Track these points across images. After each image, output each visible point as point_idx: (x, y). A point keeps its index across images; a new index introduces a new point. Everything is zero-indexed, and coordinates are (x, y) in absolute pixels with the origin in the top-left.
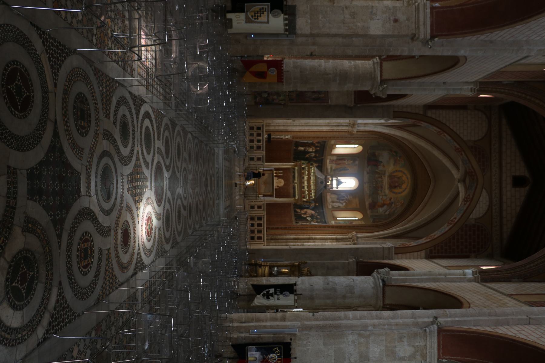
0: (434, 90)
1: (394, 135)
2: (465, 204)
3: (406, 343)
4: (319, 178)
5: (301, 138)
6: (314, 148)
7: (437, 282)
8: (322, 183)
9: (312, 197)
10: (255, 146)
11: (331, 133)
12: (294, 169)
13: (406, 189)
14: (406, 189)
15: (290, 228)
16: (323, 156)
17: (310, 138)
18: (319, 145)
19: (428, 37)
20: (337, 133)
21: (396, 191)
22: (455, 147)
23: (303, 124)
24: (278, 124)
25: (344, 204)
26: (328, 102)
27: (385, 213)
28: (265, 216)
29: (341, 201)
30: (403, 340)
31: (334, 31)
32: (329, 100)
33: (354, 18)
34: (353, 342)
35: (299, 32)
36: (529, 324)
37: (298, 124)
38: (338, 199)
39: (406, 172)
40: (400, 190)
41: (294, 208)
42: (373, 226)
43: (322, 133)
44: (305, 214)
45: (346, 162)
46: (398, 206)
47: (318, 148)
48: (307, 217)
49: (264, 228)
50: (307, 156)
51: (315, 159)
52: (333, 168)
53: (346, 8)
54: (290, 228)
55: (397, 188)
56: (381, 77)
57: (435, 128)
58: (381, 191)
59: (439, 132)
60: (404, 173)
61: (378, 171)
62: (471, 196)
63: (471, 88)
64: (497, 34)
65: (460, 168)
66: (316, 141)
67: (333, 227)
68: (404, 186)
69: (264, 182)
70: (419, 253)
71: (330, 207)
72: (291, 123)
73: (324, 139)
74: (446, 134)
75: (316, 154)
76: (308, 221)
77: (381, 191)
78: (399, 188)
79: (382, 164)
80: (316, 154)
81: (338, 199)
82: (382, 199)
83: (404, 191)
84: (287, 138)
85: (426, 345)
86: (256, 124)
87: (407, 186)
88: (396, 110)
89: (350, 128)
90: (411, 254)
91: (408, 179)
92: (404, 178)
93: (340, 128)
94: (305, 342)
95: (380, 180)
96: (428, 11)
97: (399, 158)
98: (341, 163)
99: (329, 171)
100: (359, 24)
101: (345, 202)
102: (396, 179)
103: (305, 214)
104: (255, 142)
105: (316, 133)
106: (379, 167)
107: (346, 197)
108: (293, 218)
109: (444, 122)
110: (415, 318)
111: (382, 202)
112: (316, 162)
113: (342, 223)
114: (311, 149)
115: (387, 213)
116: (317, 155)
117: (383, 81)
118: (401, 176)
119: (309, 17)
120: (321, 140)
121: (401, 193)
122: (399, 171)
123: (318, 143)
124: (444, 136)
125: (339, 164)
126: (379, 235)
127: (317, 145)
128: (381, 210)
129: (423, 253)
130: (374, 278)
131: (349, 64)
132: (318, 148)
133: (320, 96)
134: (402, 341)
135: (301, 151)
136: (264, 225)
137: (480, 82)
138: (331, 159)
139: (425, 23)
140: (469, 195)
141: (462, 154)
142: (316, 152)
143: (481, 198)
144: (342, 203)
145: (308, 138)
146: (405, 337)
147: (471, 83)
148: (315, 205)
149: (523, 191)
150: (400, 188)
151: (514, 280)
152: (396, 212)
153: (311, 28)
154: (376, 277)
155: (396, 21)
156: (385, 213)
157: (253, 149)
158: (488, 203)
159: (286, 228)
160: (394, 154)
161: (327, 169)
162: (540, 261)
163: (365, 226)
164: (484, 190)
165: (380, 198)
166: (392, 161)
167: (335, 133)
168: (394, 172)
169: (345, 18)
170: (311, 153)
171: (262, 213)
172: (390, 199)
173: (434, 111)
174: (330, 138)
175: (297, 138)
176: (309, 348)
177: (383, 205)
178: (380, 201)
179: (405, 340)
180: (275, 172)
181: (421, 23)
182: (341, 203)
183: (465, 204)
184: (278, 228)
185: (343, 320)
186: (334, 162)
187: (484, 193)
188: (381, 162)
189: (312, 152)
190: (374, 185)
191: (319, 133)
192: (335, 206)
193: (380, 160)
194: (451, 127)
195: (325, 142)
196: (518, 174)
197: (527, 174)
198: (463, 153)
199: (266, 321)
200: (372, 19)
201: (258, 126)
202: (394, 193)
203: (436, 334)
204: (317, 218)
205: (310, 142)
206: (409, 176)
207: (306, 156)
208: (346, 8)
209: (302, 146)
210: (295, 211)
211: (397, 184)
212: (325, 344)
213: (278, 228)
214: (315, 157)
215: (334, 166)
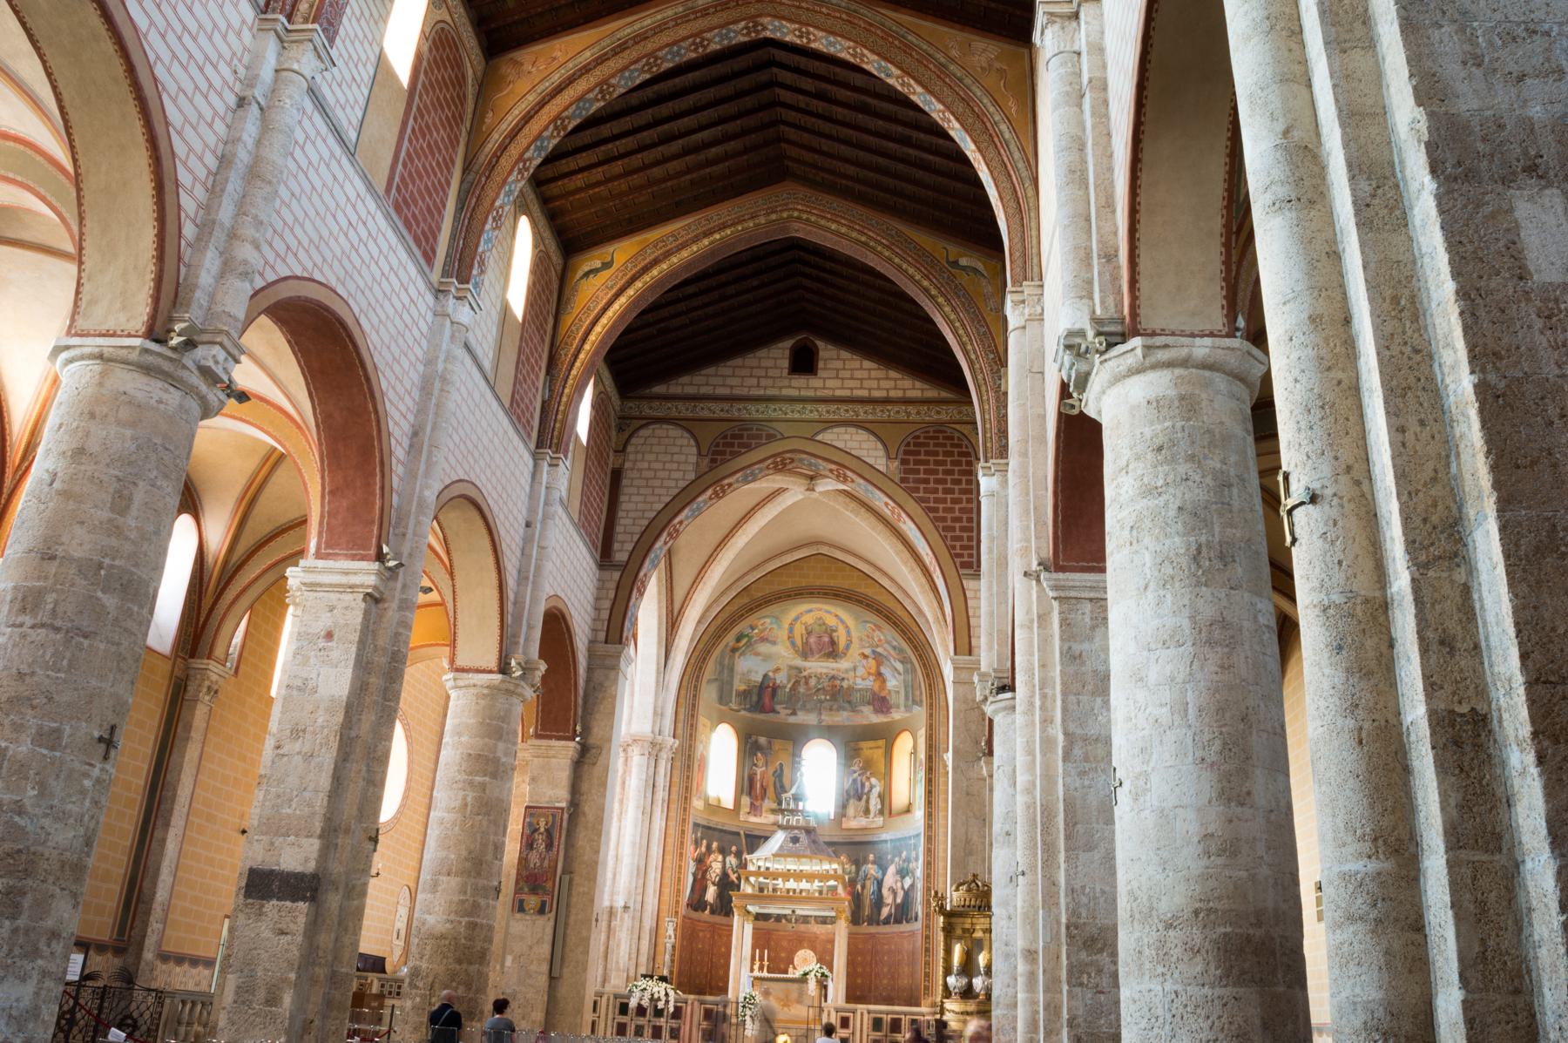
0: (543, 548)
1: (692, 640)
2: (853, 481)
3: (1086, 646)
4: (781, 847)
5: (679, 891)
6: (712, 857)
7: (1006, 558)
8: (795, 840)
9: (835, 870)
10: (674, 1023)
11: (673, 806)
12: (759, 917)
15: (927, 937)
17: (680, 867)
18: (705, 842)
19: (376, 566)
20: (675, 789)
22: (710, 499)
23: (641, 881)
24: (634, 956)
25: (873, 780)
26: (562, 809)
28: (872, 1007)
29: (866, 790)
30: (1077, 653)
31: (325, 781)
32: (557, 805)
33: (304, 731)
34: (1082, 774)
35: (311, 867)
36: (1042, 373)
37: (639, 898)
38: (860, 799)
40: (841, 628)
41: (878, 924)
42: (931, 705)
43: (671, 831)
44: (895, 893)
45: (759, 771)
47: (715, 845)
48: (903, 888)
49: (905, 1014)
52: (775, 806)
53: (278, 747)
54: (927, 937)
56: (491, 672)
57: (659, 544)
59: (670, 534)
62: (833, 467)
63: (550, 465)
64: (396, 423)
65: (777, 486)
66: (691, 852)
67: (929, 816)
68: (831, 621)
69: (784, 1006)
70: (969, 594)
71: (880, 821)
72: (633, 918)
73: (689, 828)
74: (677, 520)
76: (912, 886)
78: (834, 634)
79: (771, 674)
81: (860, 799)
83: (842, 621)
84: (675, 930)
85: (1091, 600)
86: (610, 1016)
88: (602, 636)
89: (665, 756)
90: (971, 613)
91: (811, 611)
92: (809, 619)
93: (661, 781)
94: (1084, 900)
95: (813, 682)
96: (321, 563)
100: (320, 720)
101: (868, 779)
102: (812, 640)
103: (895, 893)
104: (662, 1021)
105: (670, 848)
107: (855, 775)
108: (905, 927)
109: (646, 522)
110: (1032, 621)
111: (872, 678)
113: (920, 790)
114: (714, 864)
115: (899, 666)
116: (734, 848)
117: (504, 669)
119: (281, 839)
120: (689, 837)
122: (791, 630)
123: (697, 843)
124: (681, 523)
125: (764, 790)
127: (703, 849)
128: (893, 683)
129: (969, 584)
130: (996, 712)
131: (449, 748)
132: (715, 845)
133: (542, 830)
134: (1080, 655)
136: (898, 1013)
137: (537, 447)
139: (346, 573)
140: (831, 471)
141: (730, 485)
142: (723, 851)
143: (840, 445)
144: (872, 787)
145: (680, 873)
146: (1070, 648)
147: (535, 466)
148: (874, 862)
149: (827, 353)
150: (835, 631)
151: (1003, 388)
152: (895, 643)
153: (307, 837)
154: (993, 707)
155: (329, 636)
157: (678, 1029)
158: (852, 430)
159: (927, 950)
162: (961, 332)
163: (931, 725)
164: (819, 438)
165: (861, 684)
166: (763, 648)
167: (674, 796)
168: (793, 644)
169: (299, 753)
170: (728, 865)
171: (862, 1014)
172: (865, 657)
173: (616, 546)
174: (685, 809)
175: (677, 902)
176: (1098, 890)
177: (879, 675)
178: (869, 683)
179: (1077, 648)
180: (757, 973)
181: (344, 580)
182: (870, 791)
183: (853, 481)
184: (927, 975)
185: (1034, 798)
186: (757, 803)
187: (827, 437)
188: (765, 676)
191: (670, 840)
192: (879, 807)
193: (759, 678)
194: (659, 506)
195: (696, 825)
196: (786, 363)
197: (788, 344)
198: (726, 481)
199: (1034, 1003)
200: (315, 690)
201: (617, 1011)
202: (847, 647)
203: (1061, 575)
204: (908, 860)
205: (692, 867)
208: (278, 747)
209: (705, 889)
210: (887, 922)
211: (826, 639)
212: (1090, 848)
213: (927, 975)
214: (738, 855)
215: (769, 804)
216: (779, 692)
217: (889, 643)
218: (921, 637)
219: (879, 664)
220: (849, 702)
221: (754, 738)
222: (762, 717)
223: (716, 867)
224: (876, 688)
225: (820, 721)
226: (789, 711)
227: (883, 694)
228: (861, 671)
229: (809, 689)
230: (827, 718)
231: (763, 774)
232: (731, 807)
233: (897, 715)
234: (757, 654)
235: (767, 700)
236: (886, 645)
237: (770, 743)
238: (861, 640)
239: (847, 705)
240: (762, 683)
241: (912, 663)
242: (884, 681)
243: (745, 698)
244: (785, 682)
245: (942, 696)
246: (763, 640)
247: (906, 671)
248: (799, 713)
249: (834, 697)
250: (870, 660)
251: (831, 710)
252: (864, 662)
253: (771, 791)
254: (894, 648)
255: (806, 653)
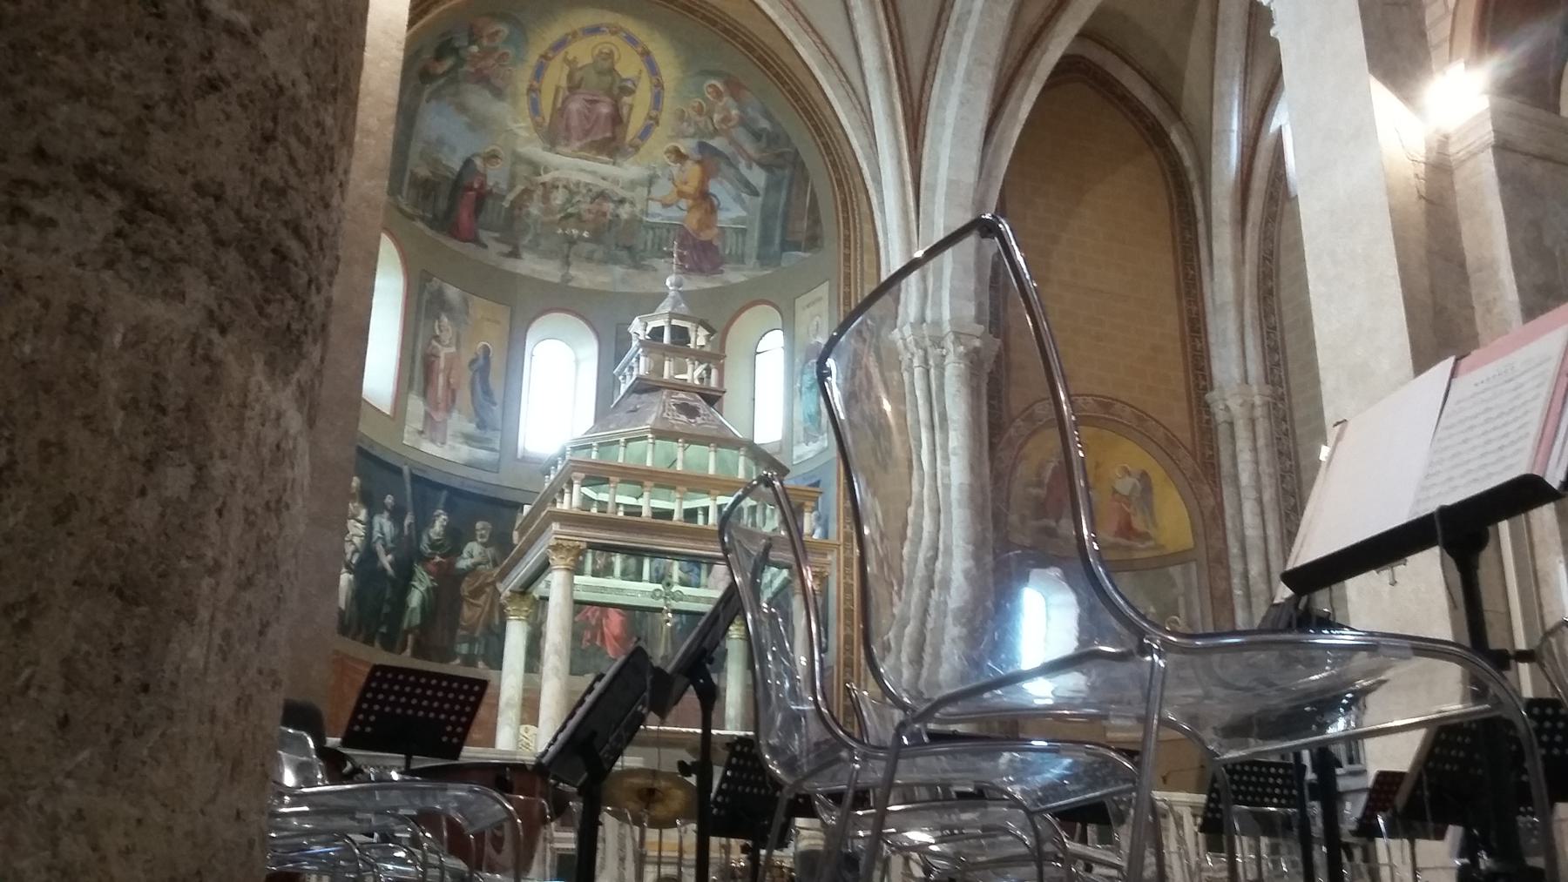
13: (646, 55)
14: (646, 55)
16: (398, 471)
21: (636, 123)
27: (754, 192)
39: (556, 32)
45: (444, 352)
46: (734, 112)
50: (386, 560)
51: (408, 520)
52: (471, 428)
55: (625, 111)
58: (622, 201)
60: (560, 45)
61: (511, 197)
68: (629, 66)
75: (384, 507)
77: (622, 201)
78: (626, 99)
79: (478, 162)
80: (384, 507)
82: (666, 205)
83: (653, 70)
87: (632, 40)
91: (595, 30)
92: (583, 52)
95: (559, 198)
97: (475, 49)
98: (448, 383)
99: (482, 454)
102: (575, 106)
106: (490, 183)
111: (684, 204)
112: (424, 521)
115: (758, 177)
116: (389, 500)
118: (566, 69)
121: (659, 86)
125: (452, 392)
126: (905, 213)
128: (732, 211)
135: (358, 594)
138: (419, 426)
142: (371, 502)
150: (631, 92)
152: (764, 124)
156: (754, 192)
160: (448, 63)
161: (469, 465)
165: (657, 213)
166: (477, 98)
168: (535, 108)
170: (376, 534)
172: (680, 156)
177: (704, 198)
178: (680, 213)
186: (438, 416)
188: (468, 163)
189: (369, 525)
190: (585, 234)
193: (456, 164)
202: (645, 133)
206: (587, 17)
207: (384, 570)
211: (604, 109)
214: (397, 515)
215: (459, 422)
216: (490, 202)
217: (744, 122)
218: (828, 112)
219: (706, 175)
220: (629, 249)
221: (436, 282)
222: (453, 244)
223: (356, 530)
224: (692, 222)
225: (566, 279)
226: (506, 249)
227: (706, 236)
228: (663, 189)
229: (548, 211)
230: (585, 277)
231: (451, 360)
232: (387, 409)
233: (734, 276)
234: (462, 109)
235: (464, 215)
236: (741, 135)
237: (465, 301)
238: (681, 116)
239: (624, 254)
240: (460, 174)
241: (798, 164)
242: (713, 210)
243: (426, 197)
244: (504, 186)
245: (867, 227)
246: (483, 79)
247: (773, 186)
248: (526, 255)
249: (596, 238)
250: (689, 164)
251: (589, 259)
252: (675, 168)
253: (464, 395)
254: (757, 135)
255: (553, 136)
